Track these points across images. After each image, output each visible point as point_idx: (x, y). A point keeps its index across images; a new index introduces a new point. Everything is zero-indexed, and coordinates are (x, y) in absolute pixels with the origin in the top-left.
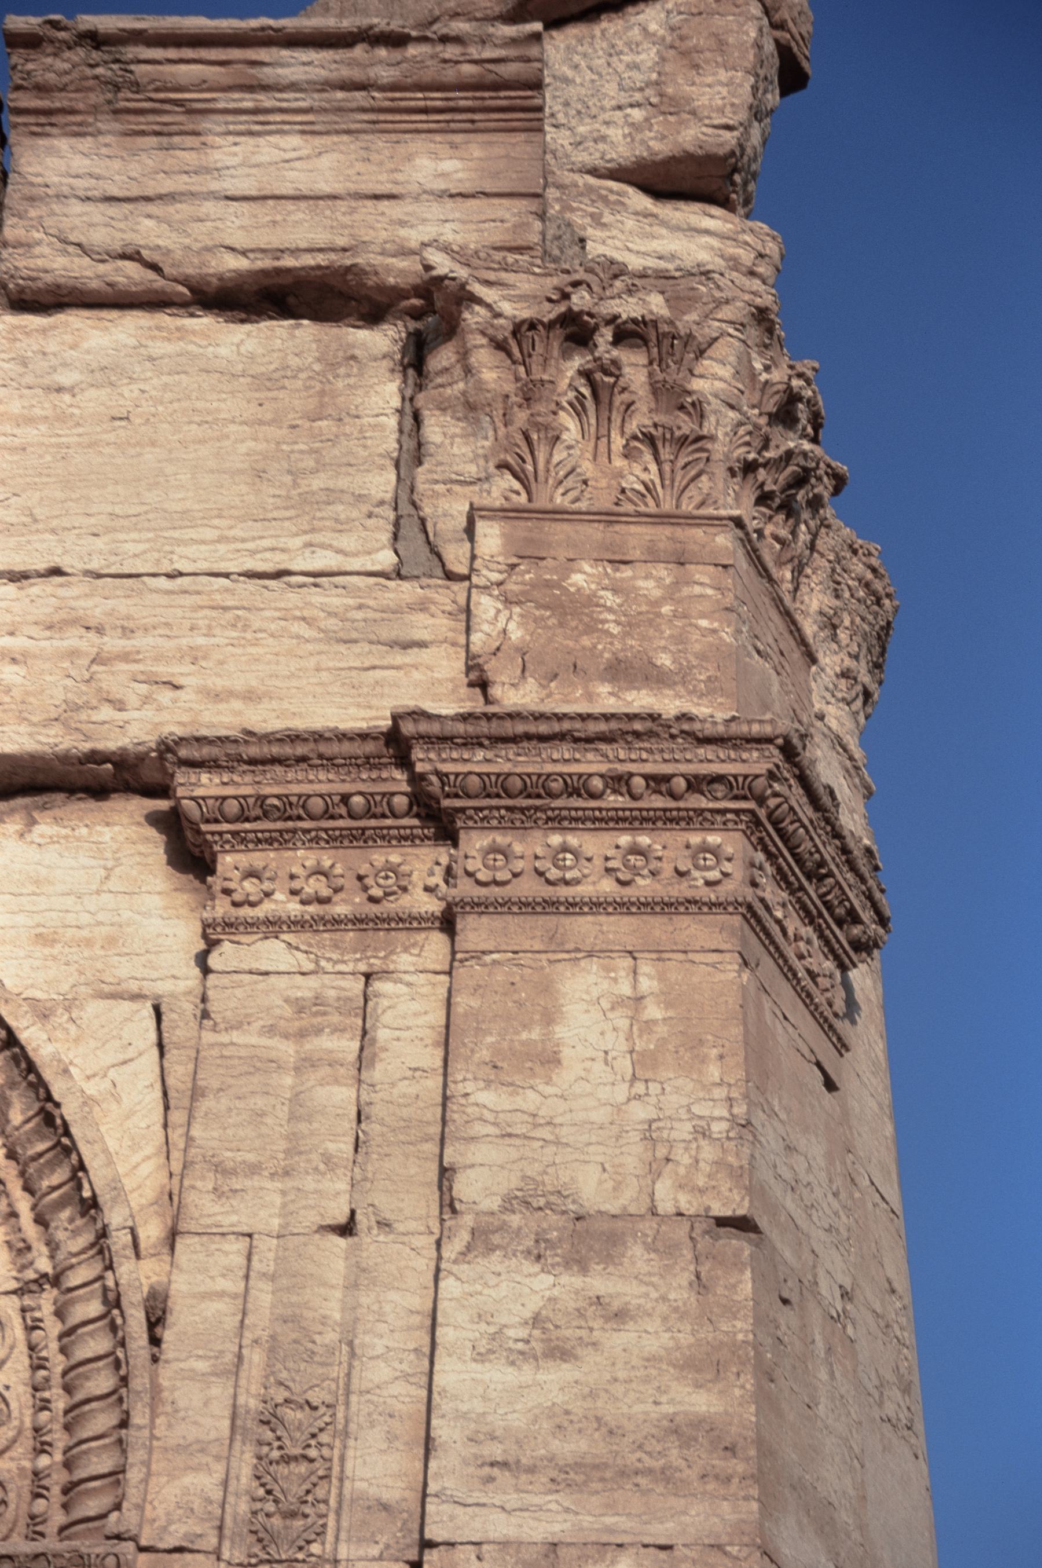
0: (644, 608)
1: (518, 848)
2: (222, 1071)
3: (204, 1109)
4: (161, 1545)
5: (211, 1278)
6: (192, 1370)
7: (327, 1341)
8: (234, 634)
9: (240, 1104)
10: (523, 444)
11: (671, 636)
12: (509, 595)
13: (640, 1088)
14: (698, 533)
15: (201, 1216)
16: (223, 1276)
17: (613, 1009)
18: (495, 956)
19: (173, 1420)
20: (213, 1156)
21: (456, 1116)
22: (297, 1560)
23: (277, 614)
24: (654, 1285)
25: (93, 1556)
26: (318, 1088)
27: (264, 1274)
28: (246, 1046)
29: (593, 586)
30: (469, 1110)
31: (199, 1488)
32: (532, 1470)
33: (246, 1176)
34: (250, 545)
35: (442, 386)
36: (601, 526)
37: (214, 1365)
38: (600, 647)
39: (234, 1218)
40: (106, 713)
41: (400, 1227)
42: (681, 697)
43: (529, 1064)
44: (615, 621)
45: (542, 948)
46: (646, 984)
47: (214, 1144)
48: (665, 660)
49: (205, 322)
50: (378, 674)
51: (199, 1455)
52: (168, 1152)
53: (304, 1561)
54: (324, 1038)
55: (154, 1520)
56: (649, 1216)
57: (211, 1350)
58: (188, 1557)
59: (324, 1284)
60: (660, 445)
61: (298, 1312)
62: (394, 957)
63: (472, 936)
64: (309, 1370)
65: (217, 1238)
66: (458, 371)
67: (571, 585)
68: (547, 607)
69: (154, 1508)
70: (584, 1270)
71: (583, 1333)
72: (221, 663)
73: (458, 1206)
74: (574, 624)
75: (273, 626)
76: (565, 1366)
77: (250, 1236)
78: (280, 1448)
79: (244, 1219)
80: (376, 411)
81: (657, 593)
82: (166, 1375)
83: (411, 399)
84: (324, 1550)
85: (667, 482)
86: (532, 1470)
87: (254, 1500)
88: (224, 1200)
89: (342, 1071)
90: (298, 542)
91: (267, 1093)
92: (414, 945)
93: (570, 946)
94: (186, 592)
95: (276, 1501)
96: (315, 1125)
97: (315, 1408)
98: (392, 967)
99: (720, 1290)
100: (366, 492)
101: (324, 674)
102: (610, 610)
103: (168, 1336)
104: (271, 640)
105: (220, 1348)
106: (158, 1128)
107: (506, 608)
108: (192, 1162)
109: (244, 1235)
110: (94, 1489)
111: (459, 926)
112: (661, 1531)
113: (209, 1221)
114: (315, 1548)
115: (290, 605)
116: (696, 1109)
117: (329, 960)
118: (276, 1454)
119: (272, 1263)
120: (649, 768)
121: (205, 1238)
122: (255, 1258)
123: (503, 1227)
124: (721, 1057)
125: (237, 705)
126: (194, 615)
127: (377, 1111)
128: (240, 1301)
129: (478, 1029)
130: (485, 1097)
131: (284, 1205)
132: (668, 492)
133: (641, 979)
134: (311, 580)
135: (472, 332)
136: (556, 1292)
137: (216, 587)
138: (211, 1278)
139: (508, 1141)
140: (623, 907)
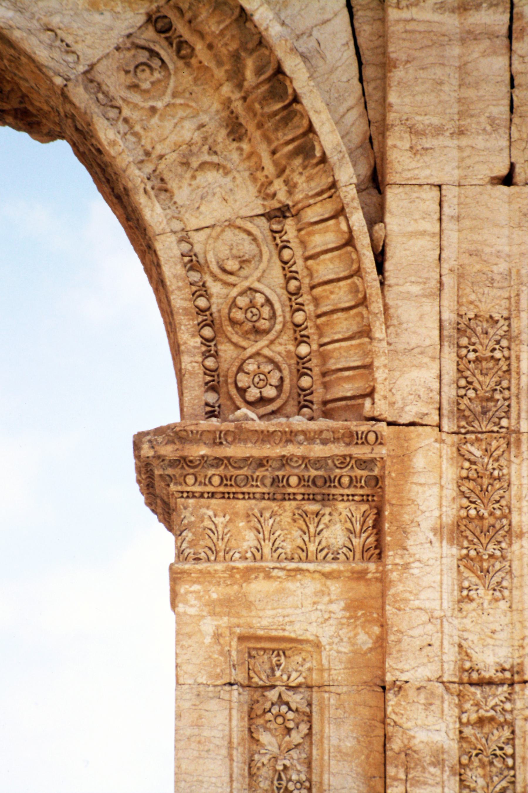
2: (407, 44)
3: (396, 79)
4: (401, 421)
5: (416, 220)
6: (408, 293)
7: (501, 270)
9: (422, 74)
15: (403, 170)
16: (424, 218)
19: (399, 331)
20: (407, 120)
22: (493, 432)
25: (360, 433)
26: (482, 59)
27: (452, 217)
28: (424, 21)
31: (423, 380)
33: (433, 136)
37: (423, 289)
39: (427, 172)
47: (407, 109)
51: (420, 356)
52: (365, 103)
53: (498, 432)
54: (483, 12)
55: (394, 403)
57: (420, 277)
58: (420, 429)
59: (496, 225)
61: (479, 248)
64: (492, 294)
65: (416, 188)
69: (393, 395)
77: (440, 186)
78: (475, 351)
79: (434, 173)
82: (390, 295)
84: (509, 423)
87: (459, 387)
88: (418, 156)
89: (498, 42)
91: (443, 64)
95: (475, 390)
96: (481, 93)
97: (497, 322)
103: (388, 266)
105: (426, 275)
106: (355, 81)
108: (392, 125)
109: (435, 185)
110: (348, 377)
113: (409, 175)
114: (504, 422)
118: (472, 356)
119: (456, 207)
121: (407, 188)
122: (445, 205)
128: (438, 237)
131: (462, 159)
138: (416, 220)
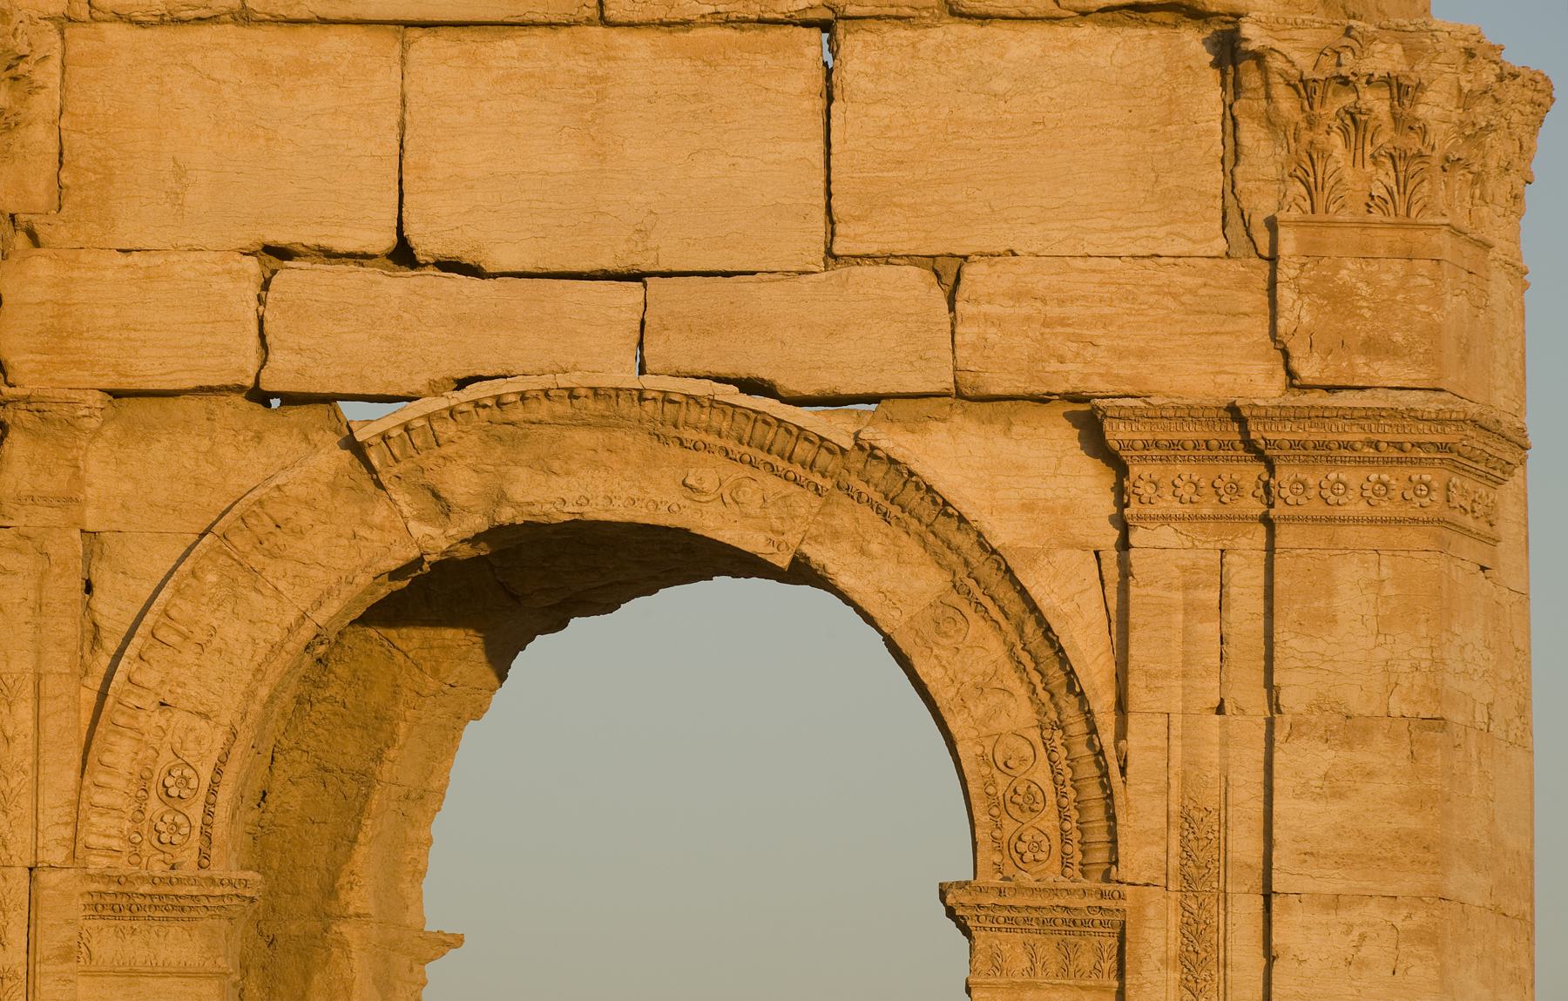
0: (1386, 297)
1: (1311, 482)
8: (1128, 306)
10: (1307, 160)
11: (1403, 318)
12: (1301, 288)
13: (1381, 639)
14: (1421, 233)
17: (1366, 588)
18: (1298, 551)
21: (1279, 655)
23: (1152, 289)
24: (1388, 758)
29: (1354, 280)
30: (1286, 651)
32: (1325, 857)
34: (1133, 234)
35: (1249, 98)
36: (1359, 230)
38: (1358, 328)
39: (1159, 704)
40: (1054, 365)
41: (1249, 712)
42: (1408, 366)
43: (1319, 623)
44: (1367, 307)
45: (1325, 547)
46: (1385, 572)
48: (1398, 337)
49: (1086, 31)
50: (1218, 339)
56: (1386, 718)
60: (1397, 160)
62: (1237, 540)
63: (1284, 538)
66: (1262, 92)
67: (1339, 279)
68: (1324, 298)
70: (1351, 749)
71: (1351, 784)
72: (1121, 327)
73: (1282, 709)
74: (1342, 310)
75: (1152, 300)
76: (1341, 802)
80: (1206, 118)
81: (1394, 284)
83: (1231, 107)
85: (1402, 190)
86: (1325, 857)
90: (1161, 232)
92: (1248, 532)
93: (1342, 546)
94: (1094, 271)
98: (1236, 547)
99: (1423, 761)
100: (1203, 189)
101: (1185, 338)
102: (1364, 298)
104: (1150, 311)
107: (1299, 298)
111: (1277, 532)
112: (1390, 890)
115: (1160, 283)
116: (1413, 653)
117: (1200, 540)
120: (1390, 438)
123: (1308, 722)
124: (1428, 620)
125: (1133, 361)
126: (1101, 290)
127: (1233, 640)
129: (1290, 599)
130: (1294, 643)
132: (1402, 195)
133: (1382, 568)
134: (1172, 260)
135: (1273, 73)
136: (1336, 760)
137: (1112, 268)
139: (1309, 670)
140: (1372, 521)
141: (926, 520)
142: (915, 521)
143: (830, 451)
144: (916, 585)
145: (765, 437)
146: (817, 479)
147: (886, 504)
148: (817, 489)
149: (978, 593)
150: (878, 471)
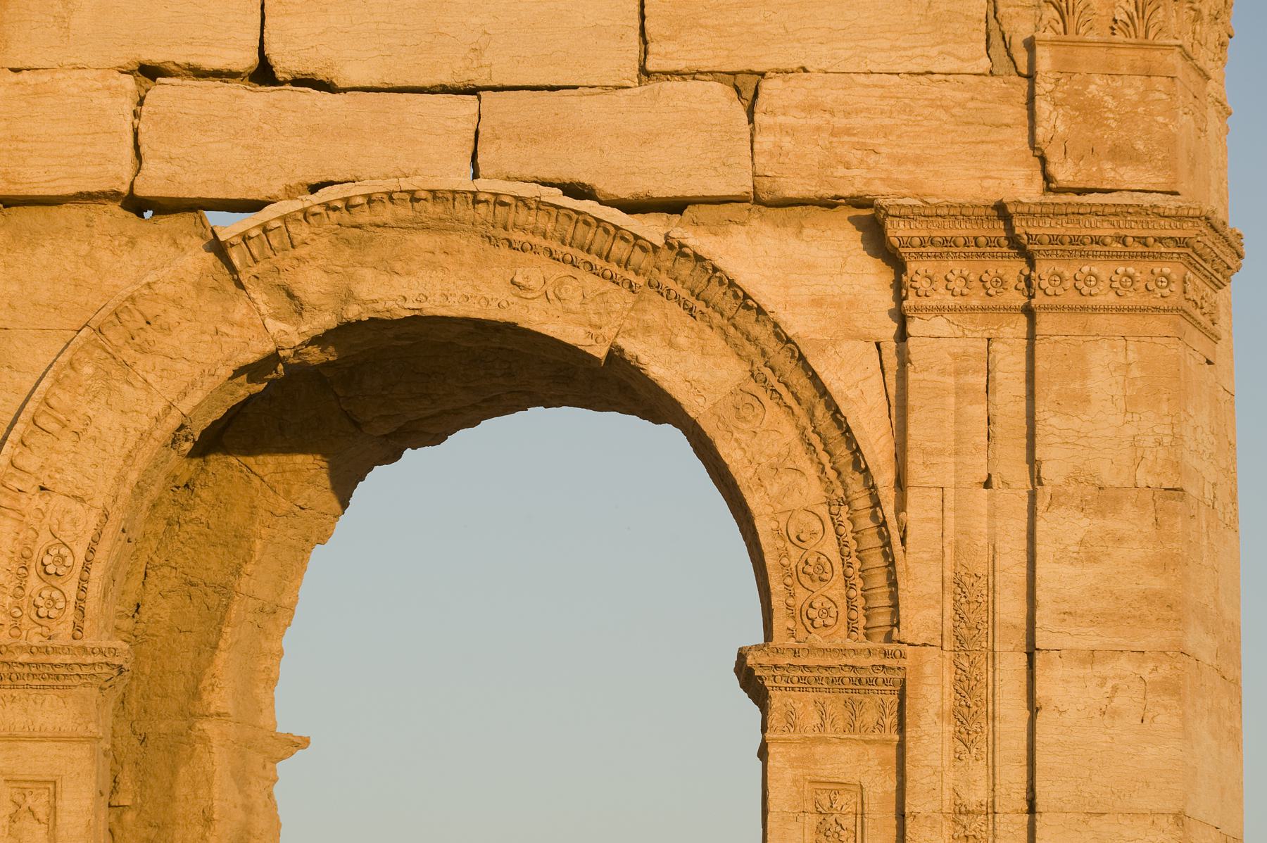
141: (728, 313)
142: (718, 316)
143: (644, 249)
144: (719, 374)
145: (585, 237)
146: (631, 276)
147: (692, 299)
148: (631, 286)
149: (773, 380)
150: (685, 268)
